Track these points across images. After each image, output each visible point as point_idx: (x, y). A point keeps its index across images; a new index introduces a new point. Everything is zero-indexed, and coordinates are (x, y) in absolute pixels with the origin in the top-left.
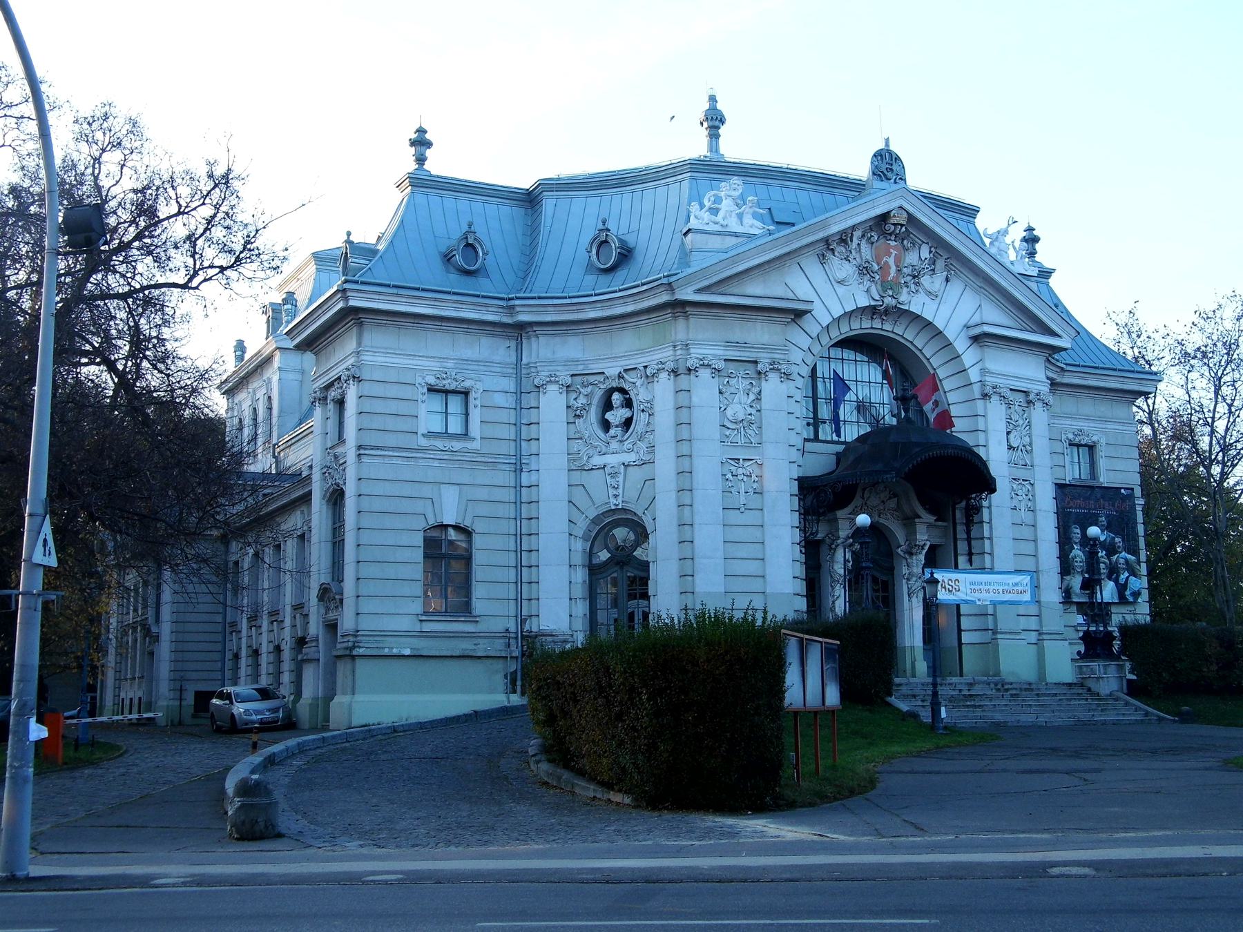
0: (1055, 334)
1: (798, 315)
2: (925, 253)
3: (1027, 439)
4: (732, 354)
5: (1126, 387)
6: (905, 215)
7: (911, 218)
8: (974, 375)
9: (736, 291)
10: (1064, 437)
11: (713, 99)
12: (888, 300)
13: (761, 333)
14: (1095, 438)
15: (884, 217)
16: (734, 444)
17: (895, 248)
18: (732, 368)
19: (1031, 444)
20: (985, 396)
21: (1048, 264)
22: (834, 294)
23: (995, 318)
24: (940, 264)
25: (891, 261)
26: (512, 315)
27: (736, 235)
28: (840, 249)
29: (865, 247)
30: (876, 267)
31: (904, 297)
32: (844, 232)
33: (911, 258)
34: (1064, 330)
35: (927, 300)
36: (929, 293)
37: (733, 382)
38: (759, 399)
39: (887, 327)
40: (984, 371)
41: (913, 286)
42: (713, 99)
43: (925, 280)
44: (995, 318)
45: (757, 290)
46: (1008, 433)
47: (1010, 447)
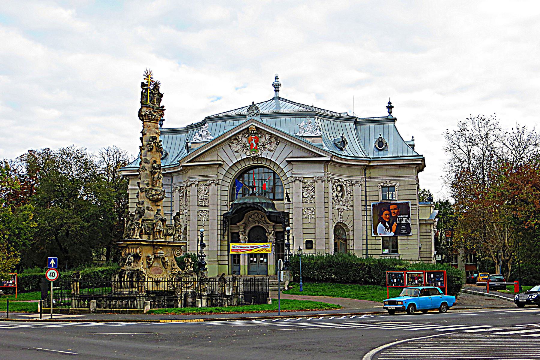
0: (321, 156)
1: (220, 165)
2: (267, 137)
3: (313, 194)
4: (201, 179)
5: (405, 163)
6: (254, 127)
7: (257, 128)
8: (288, 175)
9: (203, 160)
10: (378, 185)
11: (277, 78)
12: (252, 155)
13: (210, 172)
14: (394, 184)
15: (248, 128)
16: (202, 206)
17: (254, 138)
18: (201, 183)
19: (315, 195)
20: (293, 182)
21: (394, 117)
22: (233, 156)
23: (297, 155)
24: (273, 140)
25: (253, 142)
26: (165, 171)
27: (203, 142)
28: (235, 141)
29: (243, 139)
30: (248, 145)
31: (259, 153)
32: (235, 135)
33: (263, 140)
34: (326, 154)
35: (269, 152)
36: (269, 150)
37: (201, 187)
38: (208, 192)
39: (259, 162)
40: (293, 173)
41: (263, 149)
42: (277, 78)
43: (268, 146)
44: (297, 155)
45: (208, 159)
46: (303, 193)
47: (303, 197)
